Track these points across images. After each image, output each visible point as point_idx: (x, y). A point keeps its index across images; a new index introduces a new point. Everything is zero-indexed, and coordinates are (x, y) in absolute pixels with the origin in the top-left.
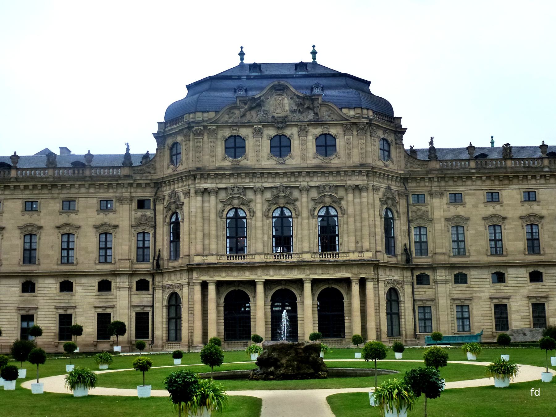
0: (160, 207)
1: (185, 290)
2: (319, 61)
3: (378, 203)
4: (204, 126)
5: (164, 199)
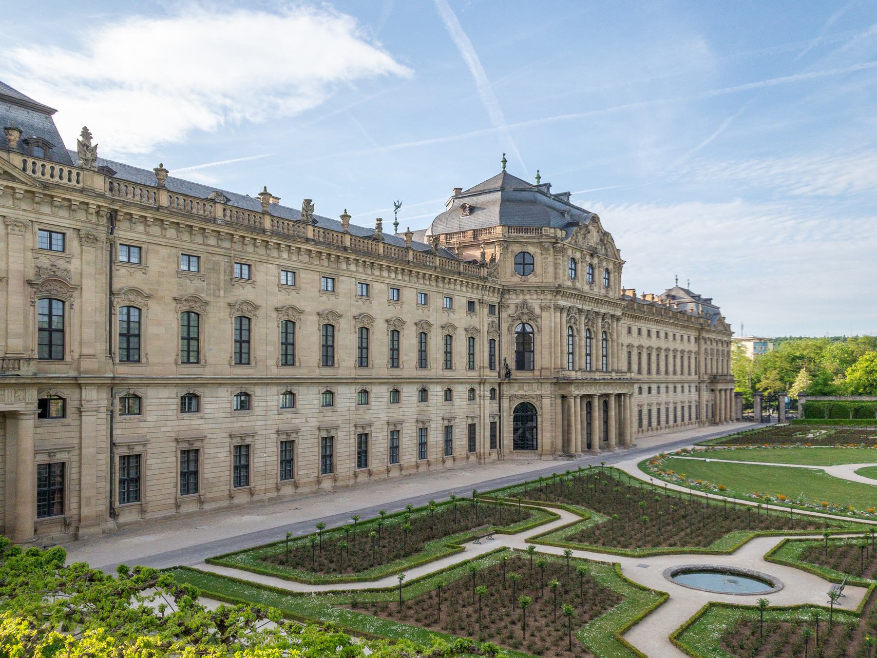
0: (504, 315)
5: (508, 307)
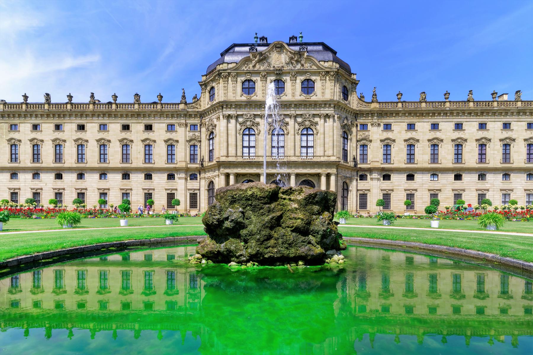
0: (204, 130)
4: (228, 73)
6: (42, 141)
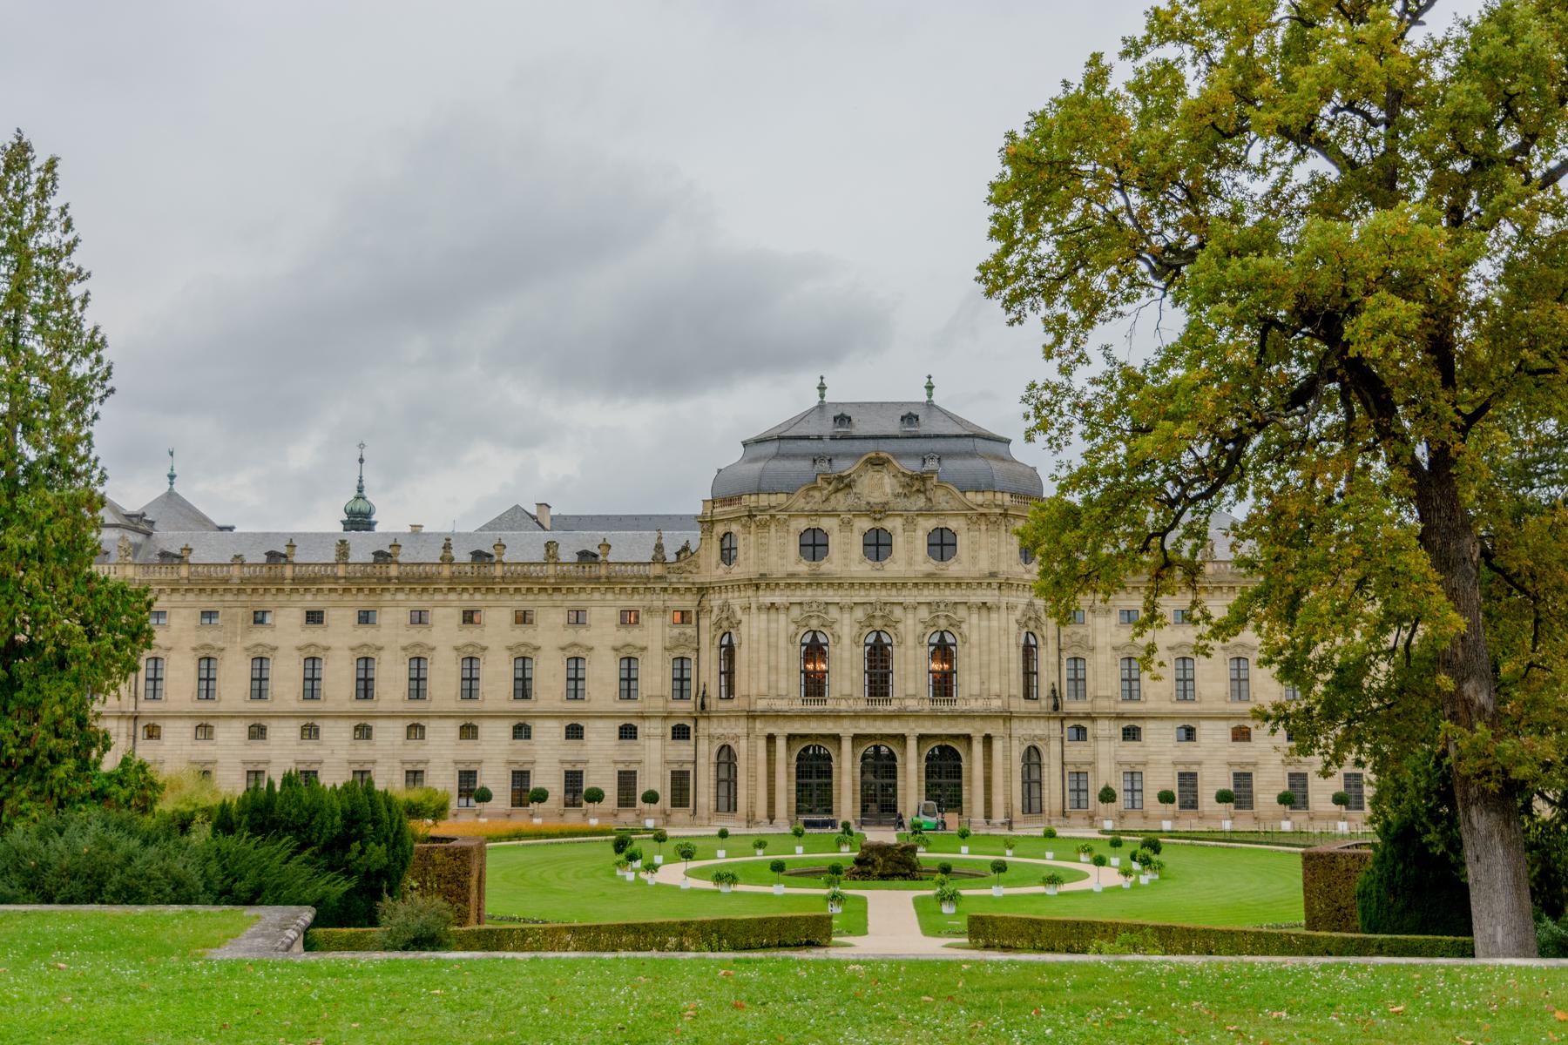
1: (743, 743)
2: (937, 399)
3: (1014, 627)
6: (327, 649)
